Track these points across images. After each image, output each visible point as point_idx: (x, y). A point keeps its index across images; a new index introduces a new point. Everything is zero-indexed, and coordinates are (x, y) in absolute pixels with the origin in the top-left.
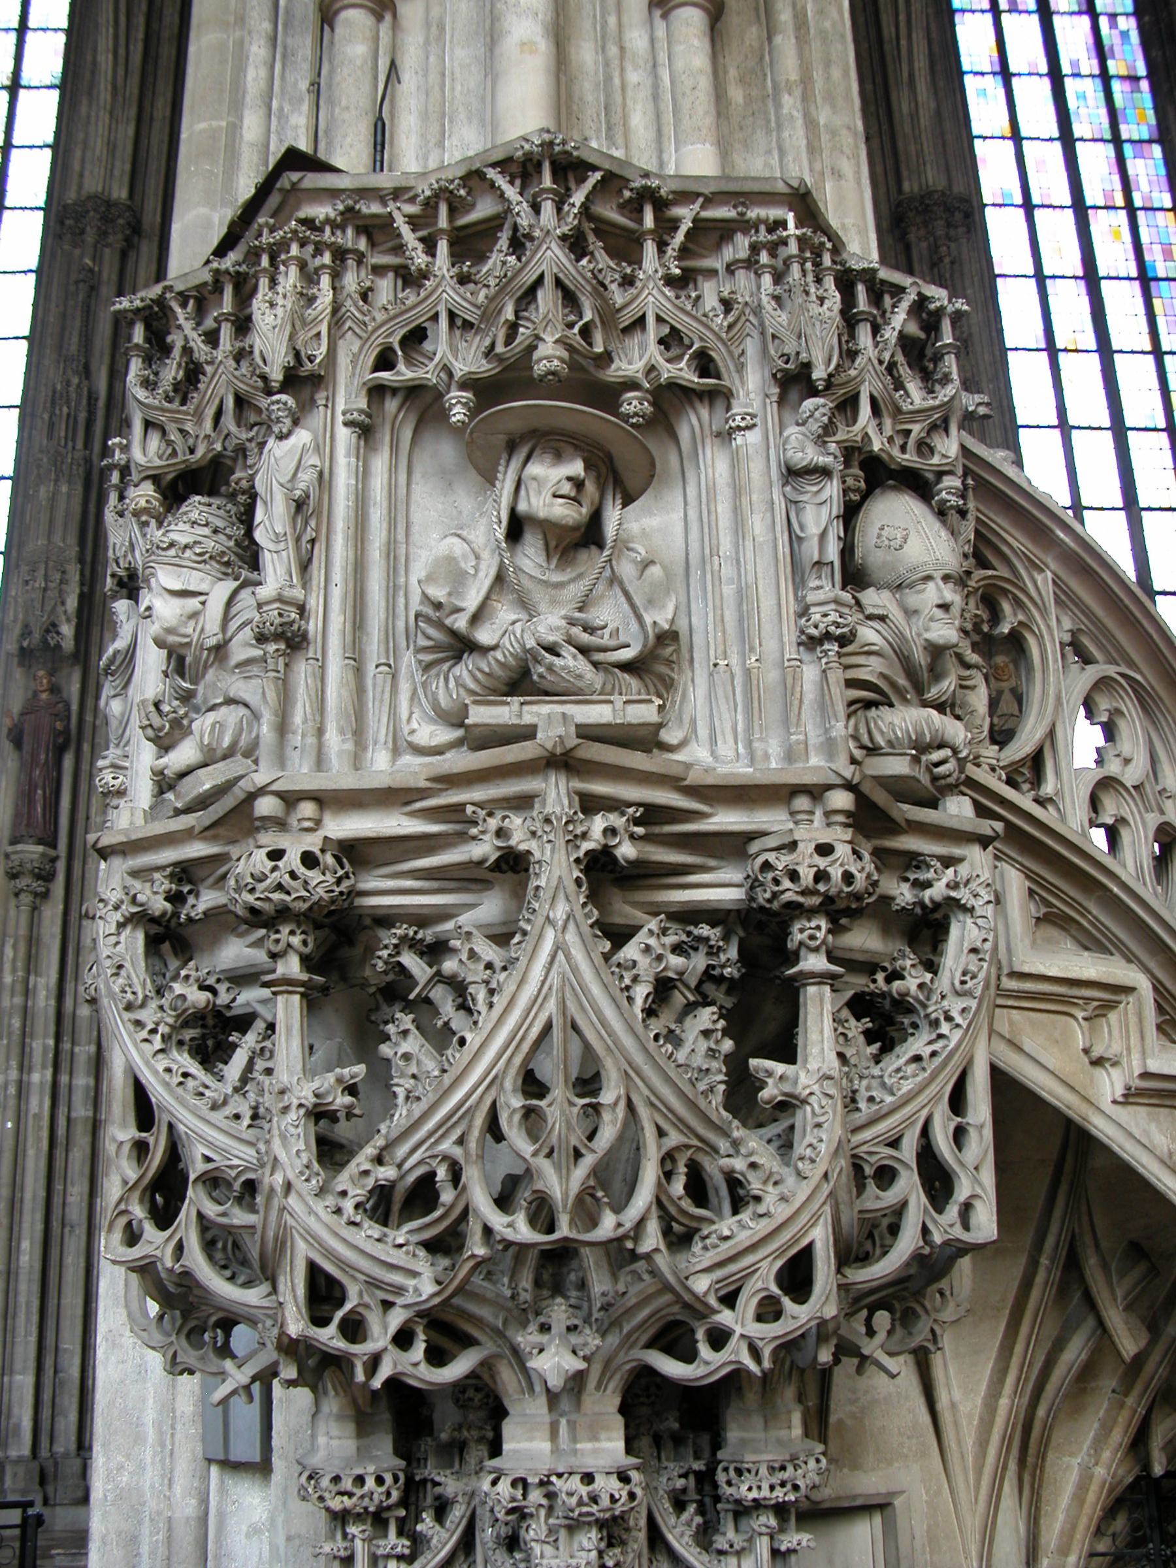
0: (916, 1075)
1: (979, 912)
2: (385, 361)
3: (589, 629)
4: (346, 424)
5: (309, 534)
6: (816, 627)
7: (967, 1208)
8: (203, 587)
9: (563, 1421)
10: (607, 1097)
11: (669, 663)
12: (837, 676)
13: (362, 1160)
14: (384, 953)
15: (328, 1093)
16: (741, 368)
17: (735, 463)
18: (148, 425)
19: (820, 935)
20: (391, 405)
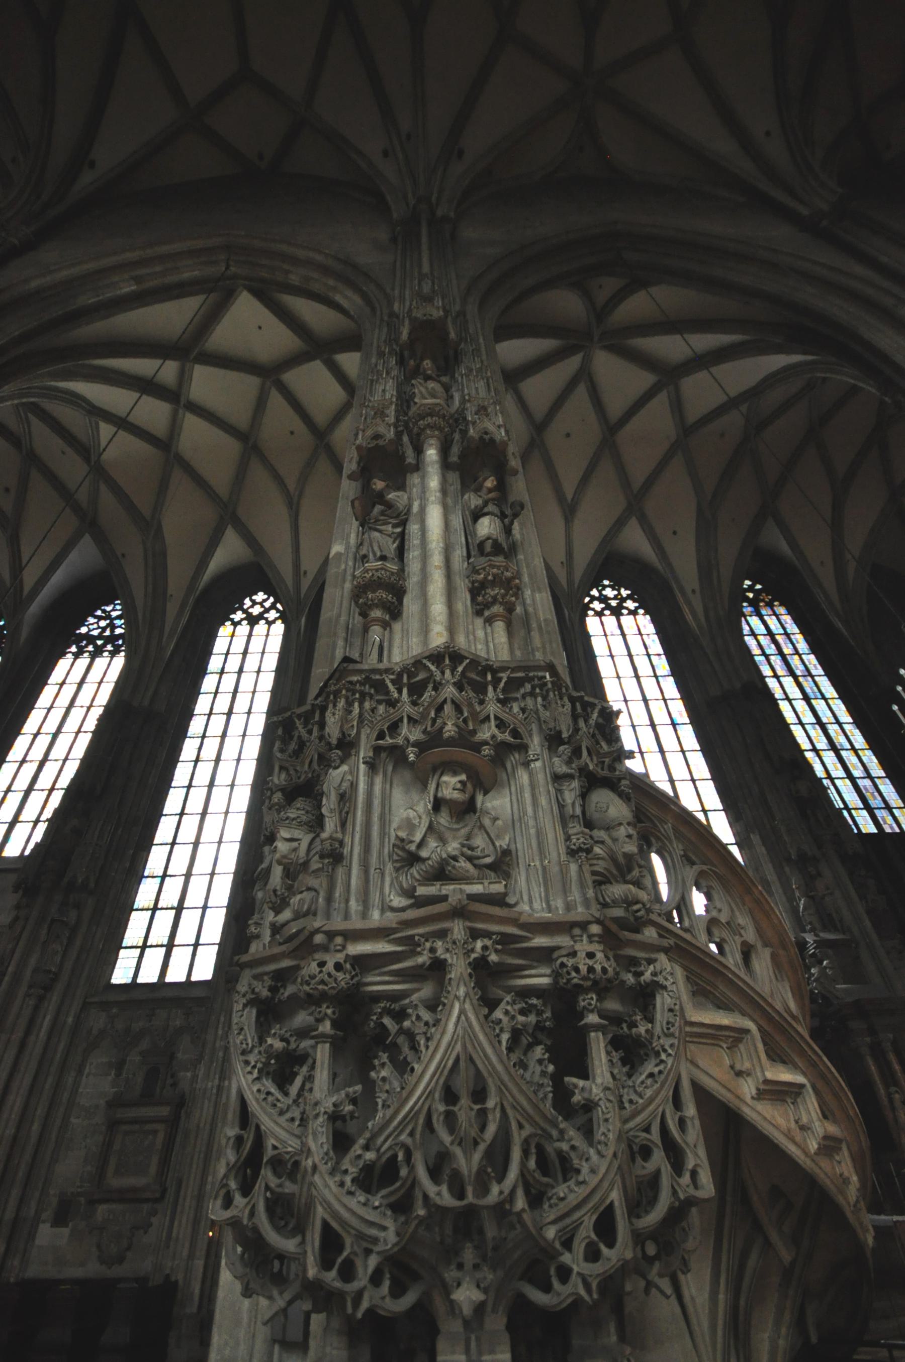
0: (652, 1086)
1: (669, 988)
2: (381, 736)
3: (471, 849)
4: (364, 763)
5: (346, 809)
6: (574, 845)
7: (694, 1174)
8: (300, 837)
9: (473, 1337)
10: (490, 1103)
11: (508, 865)
12: (586, 868)
13: (357, 1149)
14: (374, 1018)
15: (341, 1103)
16: (531, 735)
17: (531, 775)
18: (282, 768)
19: (593, 1002)
20: (383, 755)
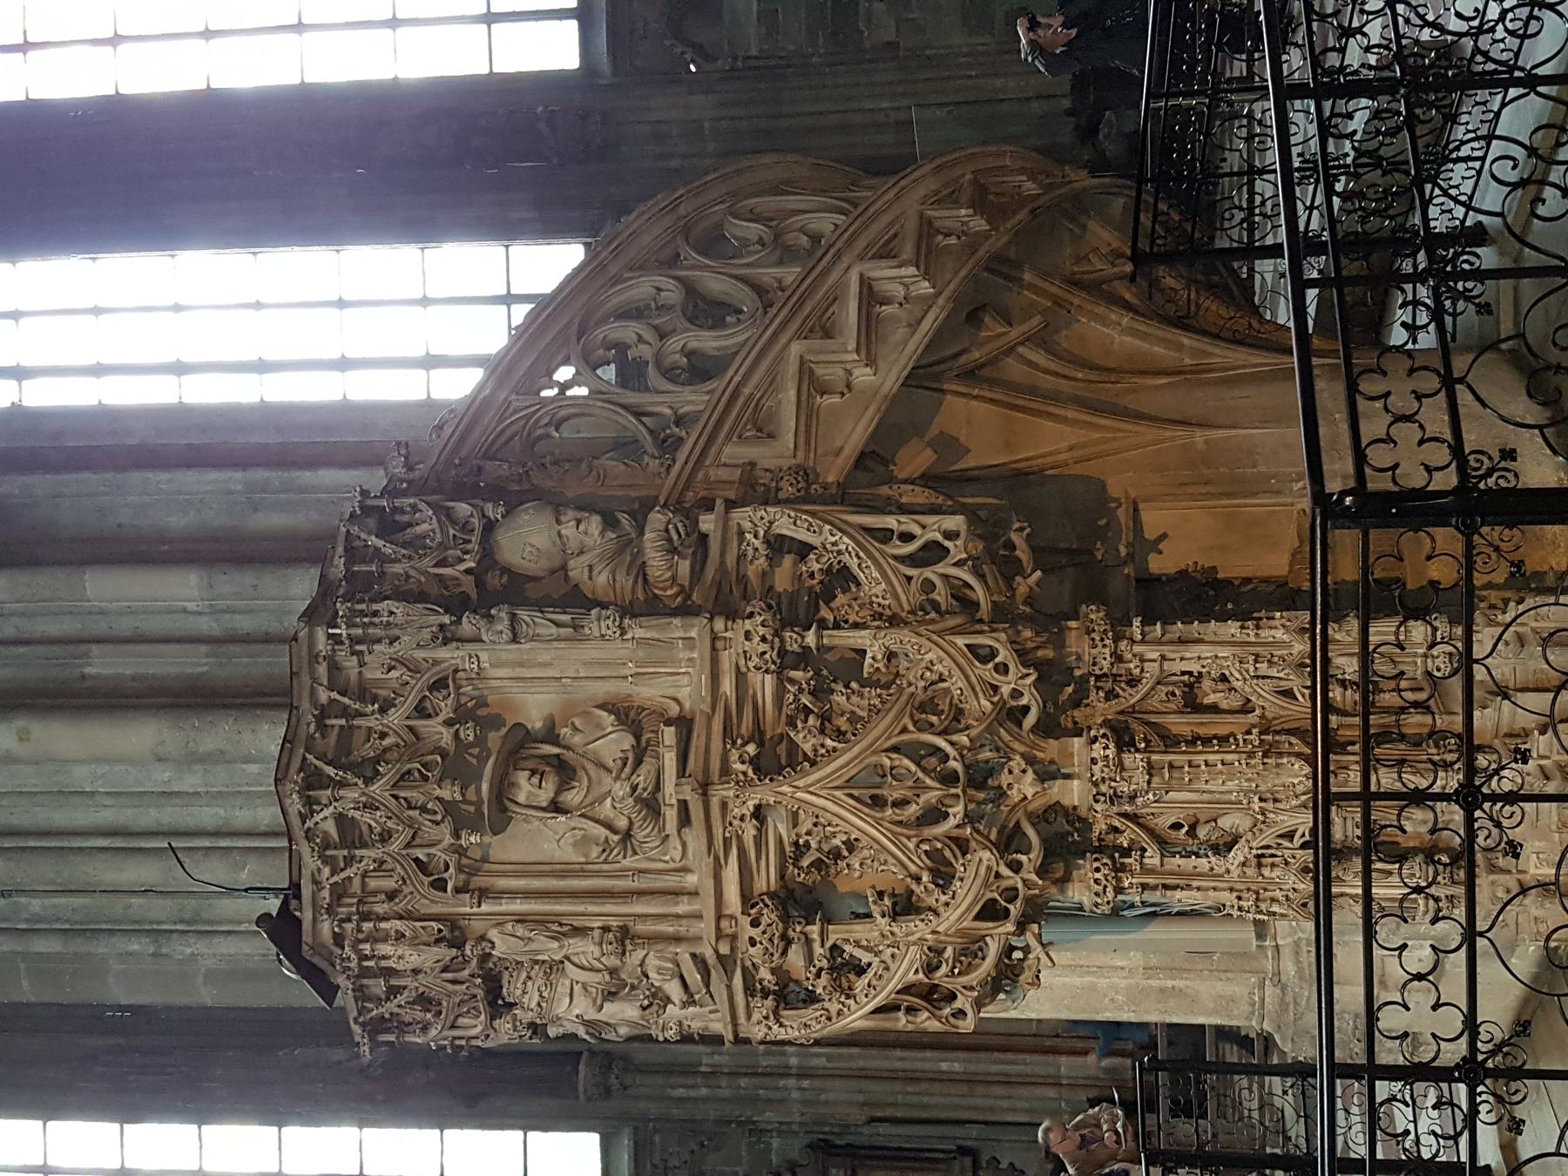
2: (440, 885)
8: (568, 983)
16: (436, 662)
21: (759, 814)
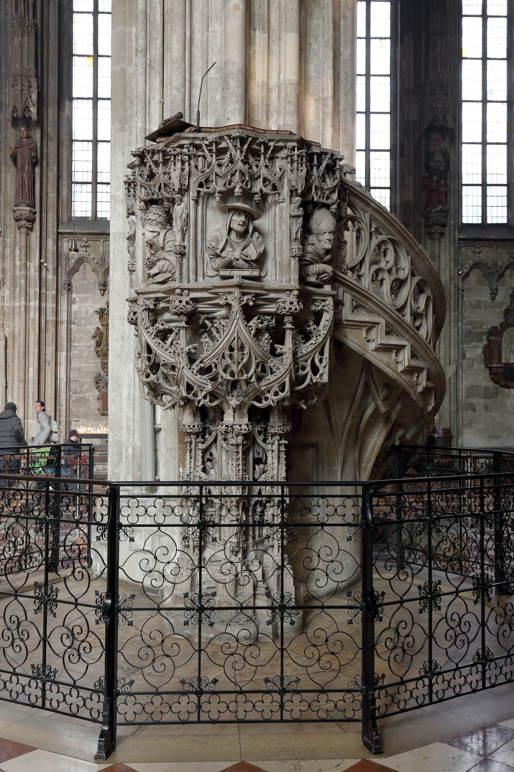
2: (201, 185)
10: (245, 352)
13: (198, 362)
21: (228, 306)
